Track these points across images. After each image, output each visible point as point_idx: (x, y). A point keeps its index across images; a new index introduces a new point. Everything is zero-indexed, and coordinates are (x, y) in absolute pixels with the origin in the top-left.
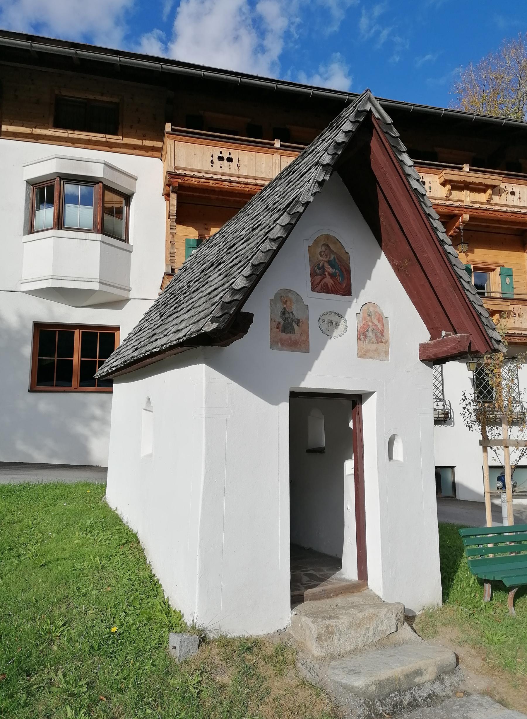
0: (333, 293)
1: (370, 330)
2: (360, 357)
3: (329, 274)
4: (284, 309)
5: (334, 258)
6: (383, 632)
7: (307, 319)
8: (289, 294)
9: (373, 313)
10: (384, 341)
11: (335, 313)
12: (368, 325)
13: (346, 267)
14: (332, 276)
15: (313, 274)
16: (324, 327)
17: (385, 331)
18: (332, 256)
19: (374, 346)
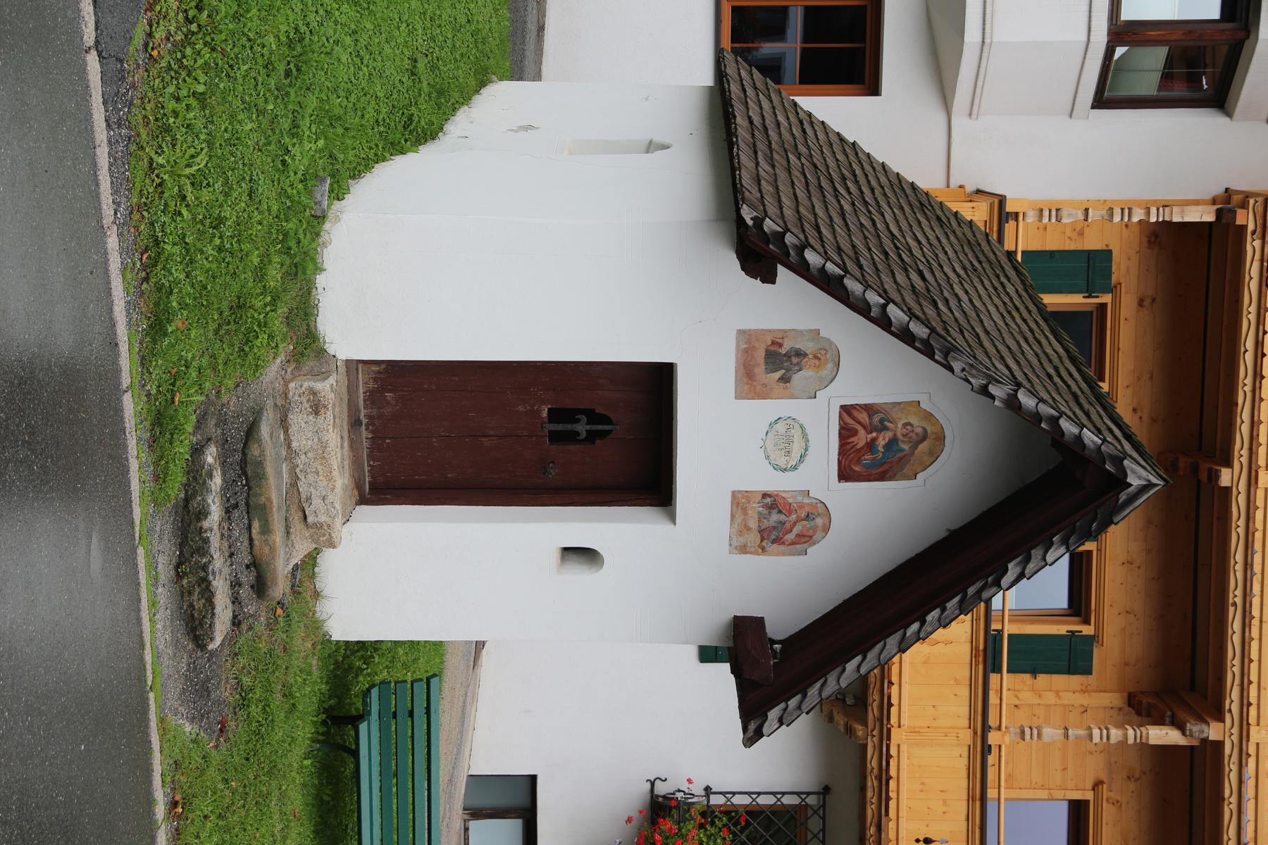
0: (842, 446)
1: (782, 517)
2: (733, 493)
3: (874, 440)
4: (805, 355)
5: (902, 450)
6: (309, 499)
7: (793, 397)
8: (830, 366)
9: (812, 523)
10: (764, 544)
11: (806, 450)
12: (790, 513)
13: (890, 474)
14: (871, 445)
15: (869, 409)
16: (781, 427)
17: (782, 548)
18: (906, 447)
19: (753, 524)
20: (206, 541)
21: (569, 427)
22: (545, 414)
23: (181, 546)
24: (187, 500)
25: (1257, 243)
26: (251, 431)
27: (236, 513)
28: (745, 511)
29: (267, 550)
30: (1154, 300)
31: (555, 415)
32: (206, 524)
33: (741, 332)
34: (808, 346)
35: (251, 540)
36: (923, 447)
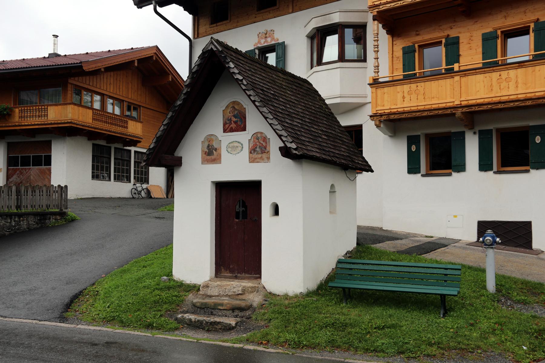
1: (258, 147)
3: (234, 122)
6: (234, 292)
8: (212, 137)
14: (235, 123)
15: (224, 125)
16: (229, 150)
17: (268, 146)
18: (236, 112)
19: (260, 156)
20: (198, 321)
21: (241, 213)
22: (237, 220)
23: (199, 328)
24: (187, 324)
25: (381, 7)
26: (194, 305)
27: (215, 313)
28: (256, 159)
29: (228, 305)
30: (417, 31)
31: (238, 218)
32: (193, 320)
33: (202, 163)
34: (206, 144)
35: (224, 310)
36: (236, 107)
